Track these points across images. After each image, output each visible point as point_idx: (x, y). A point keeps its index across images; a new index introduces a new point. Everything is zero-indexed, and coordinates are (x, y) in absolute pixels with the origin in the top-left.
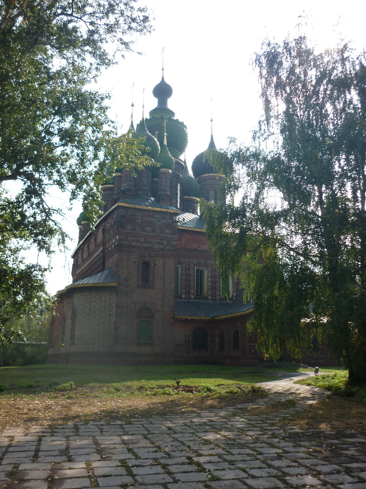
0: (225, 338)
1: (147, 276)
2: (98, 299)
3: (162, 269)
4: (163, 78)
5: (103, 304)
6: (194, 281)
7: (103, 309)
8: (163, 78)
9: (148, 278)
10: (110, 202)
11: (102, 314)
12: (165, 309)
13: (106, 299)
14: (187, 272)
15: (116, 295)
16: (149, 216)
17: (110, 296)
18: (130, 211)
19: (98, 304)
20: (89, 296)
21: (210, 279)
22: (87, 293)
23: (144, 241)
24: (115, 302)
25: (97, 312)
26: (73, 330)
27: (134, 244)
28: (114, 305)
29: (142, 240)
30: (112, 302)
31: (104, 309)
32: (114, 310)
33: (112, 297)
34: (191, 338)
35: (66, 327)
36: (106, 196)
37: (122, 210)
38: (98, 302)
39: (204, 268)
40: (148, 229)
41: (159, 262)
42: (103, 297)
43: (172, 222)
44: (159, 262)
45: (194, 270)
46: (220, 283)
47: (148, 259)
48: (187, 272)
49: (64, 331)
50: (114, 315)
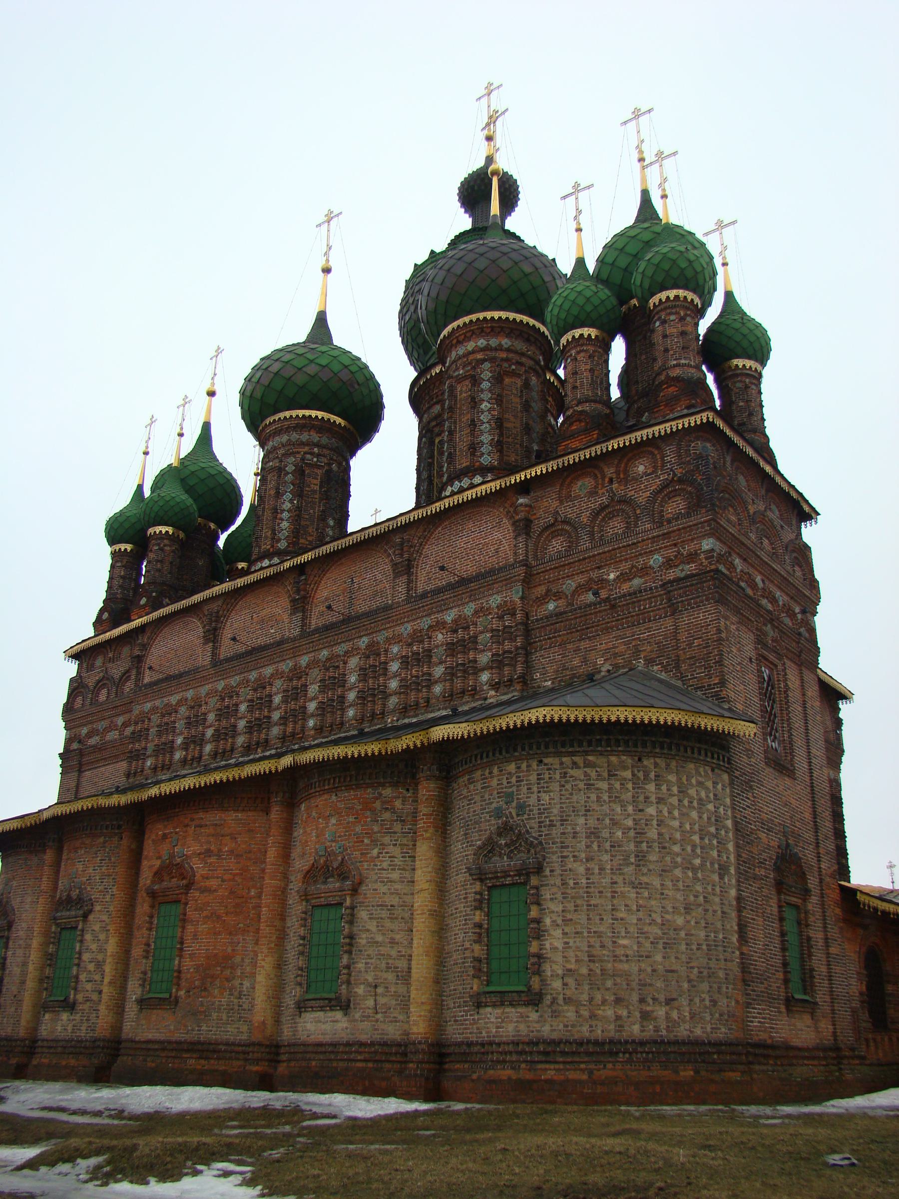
2: (675, 789)
5: (694, 814)
7: (696, 838)
10: (319, 472)
11: (697, 862)
15: (731, 783)
19: (676, 813)
20: (628, 774)
22: (613, 759)
25: (676, 848)
31: (701, 838)
32: (731, 846)
35: (363, 914)
36: (306, 449)
37: (708, 445)
38: (674, 801)
42: (694, 781)
49: (351, 937)
50: (732, 871)
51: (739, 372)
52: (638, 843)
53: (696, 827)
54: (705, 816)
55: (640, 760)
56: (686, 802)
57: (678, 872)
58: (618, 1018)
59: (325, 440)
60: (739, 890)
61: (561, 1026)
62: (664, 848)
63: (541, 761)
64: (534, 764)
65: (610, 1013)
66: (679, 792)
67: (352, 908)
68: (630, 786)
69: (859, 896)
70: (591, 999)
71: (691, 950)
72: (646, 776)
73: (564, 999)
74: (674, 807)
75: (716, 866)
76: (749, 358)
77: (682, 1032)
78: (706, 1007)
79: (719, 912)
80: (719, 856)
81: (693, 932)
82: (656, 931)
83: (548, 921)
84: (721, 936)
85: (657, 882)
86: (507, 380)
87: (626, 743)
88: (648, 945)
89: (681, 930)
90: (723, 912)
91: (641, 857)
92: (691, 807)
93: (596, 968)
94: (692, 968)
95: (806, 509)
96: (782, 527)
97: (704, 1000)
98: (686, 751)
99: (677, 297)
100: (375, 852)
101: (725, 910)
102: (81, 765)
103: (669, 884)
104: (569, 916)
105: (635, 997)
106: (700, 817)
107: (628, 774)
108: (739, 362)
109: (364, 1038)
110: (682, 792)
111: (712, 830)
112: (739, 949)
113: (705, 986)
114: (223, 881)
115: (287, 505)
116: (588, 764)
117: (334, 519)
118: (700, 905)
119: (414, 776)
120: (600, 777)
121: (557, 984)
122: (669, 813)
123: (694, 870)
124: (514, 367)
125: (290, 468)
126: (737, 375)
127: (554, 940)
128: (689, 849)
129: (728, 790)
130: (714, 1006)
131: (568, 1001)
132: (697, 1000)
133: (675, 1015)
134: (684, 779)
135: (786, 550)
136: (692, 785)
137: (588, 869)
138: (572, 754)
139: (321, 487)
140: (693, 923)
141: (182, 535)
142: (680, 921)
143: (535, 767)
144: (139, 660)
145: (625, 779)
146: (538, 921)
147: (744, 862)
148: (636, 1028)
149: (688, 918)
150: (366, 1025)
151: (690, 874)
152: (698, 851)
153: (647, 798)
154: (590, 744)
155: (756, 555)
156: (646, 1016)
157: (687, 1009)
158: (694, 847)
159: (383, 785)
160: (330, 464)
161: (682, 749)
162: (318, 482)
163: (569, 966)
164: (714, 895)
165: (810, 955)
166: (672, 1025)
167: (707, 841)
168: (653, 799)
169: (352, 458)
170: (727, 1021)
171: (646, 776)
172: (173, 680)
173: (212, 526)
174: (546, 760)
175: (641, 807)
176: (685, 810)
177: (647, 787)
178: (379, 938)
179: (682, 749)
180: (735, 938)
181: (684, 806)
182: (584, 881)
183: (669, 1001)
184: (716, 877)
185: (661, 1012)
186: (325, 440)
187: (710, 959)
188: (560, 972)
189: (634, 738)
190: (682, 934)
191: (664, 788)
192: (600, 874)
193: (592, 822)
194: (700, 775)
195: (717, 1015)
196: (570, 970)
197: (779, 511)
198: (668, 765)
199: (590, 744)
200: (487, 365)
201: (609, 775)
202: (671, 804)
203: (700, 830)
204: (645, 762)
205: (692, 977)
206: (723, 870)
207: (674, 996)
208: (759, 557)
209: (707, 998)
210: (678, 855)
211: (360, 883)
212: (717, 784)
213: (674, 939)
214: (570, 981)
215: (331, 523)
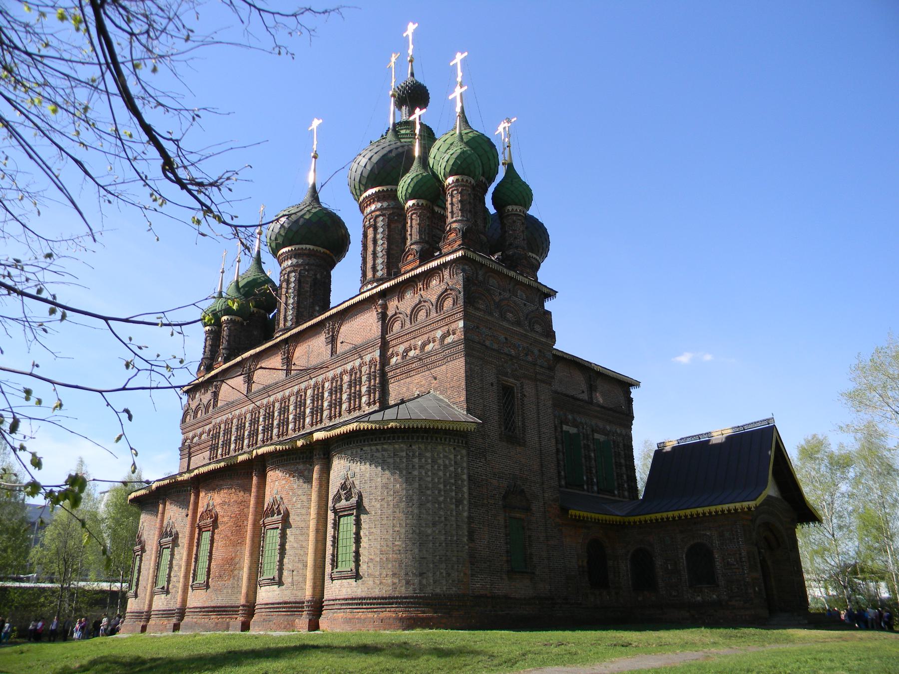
2: (430, 461)
3: (534, 407)
4: (412, 75)
5: (441, 474)
7: (441, 486)
11: (441, 499)
13: (447, 462)
15: (468, 454)
17: (455, 456)
19: (430, 473)
22: (397, 446)
24: (465, 471)
25: (429, 492)
27: (488, 343)
28: (465, 477)
29: (502, 338)
30: (459, 470)
31: (445, 486)
32: (465, 489)
34: (585, 564)
37: (466, 267)
38: (429, 467)
40: (509, 315)
41: (529, 389)
50: (465, 502)
51: (510, 213)
53: (442, 480)
54: (448, 474)
55: (411, 446)
57: (429, 505)
60: (469, 513)
61: (366, 589)
62: (422, 492)
63: (362, 449)
64: (359, 450)
66: (432, 462)
68: (404, 460)
70: (381, 574)
71: (436, 546)
72: (413, 455)
73: (368, 575)
75: (454, 500)
76: (516, 204)
78: (443, 577)
79: (455, 526)
80: (456, 495)
81: (437, 537)
84: (455, 538)
86: (393, 226)
87: (403, 438)
89: (429, 536)
90: (457, 525)
92: (439, 469)
94: (436, 556)
95: (546, 291)
96: (525, 305)
97: (442, 573)
98: (437, 440)
100: (294, 499)
101: (459, 524)
102: (190, 454)
103: (424, 511)
104: (372, 530)
106: (445, 475)
107: (404, 454)
108: (510, 208)
110: (434, 461)
111: (453, 481)
112: (467, 545)
113: (443, 566)
114: (231, 517)
117: (319, 306)
118: (442, 522)
119: (311, 458)
120: (390, 457)
122: (426, 473)
123: (439, 503)
124: (396, 218)
125: (293, 279)
126: (508, 215)
128: (436, 492)
129: (465, 459)
130: (449, 576)
132: (438, 573)
133: (424, 582)
134: (435, 455)
135: (526, 318)
136: (440, 458)
137: (381, 505)
138: (376, 445)
139: (311, 289)
140: (437, 532)
142: (429, 531)
143: (359, 452)
144: (216, 395)
145: (402, 457)
147: (474, 497)
149: (434, 529)
151: (437, 506)
152: (443, 493)
153: (413, 466)
154: (384, 440)
155: (500, 324)
157: (432, 578)
158: (440, 491)
159: (298, 463)
160: (315, 275)
161: (434, 439)
162: (308, 286)
163: (371, 557)
164: (451, 516)
167: (448, 487)
168: (417, 466)
169: (331, 270)
170: (457, 584)
171: (413, 455)
172: (230, 405)
173: (262, 311)
174: (364, 449)
175: (410, 471)
176: (435, 472)
177: (414, 460)
178: (295, 545)
179: (434, 439)
180: (465, 539)
181: (435, 469)
182: (380, 512)
184: (453, 507)
187: (447, 551)
188: (366, 560)
189: (407, 435)
190: (431, 538)
191: (423, 460)
192: (387, 507)
194: (446, 452)
195: (450, 581)
196: (371, 559)
197: (526, 295)
198: (426, 448)
199: (384, 440)
200: (381, 218)
201: (394, 455)
202: (427, 469)
203: (444, 481)
204: (413, 447)
205: (435, 561)
206: (459, 502)
207: (424, 572)
208: (502, 325)
209: (444, 572)
210: (430, 496)
212: (458, 456)
213: (426, 541)
214: (370, 564)
215: (317, 308)
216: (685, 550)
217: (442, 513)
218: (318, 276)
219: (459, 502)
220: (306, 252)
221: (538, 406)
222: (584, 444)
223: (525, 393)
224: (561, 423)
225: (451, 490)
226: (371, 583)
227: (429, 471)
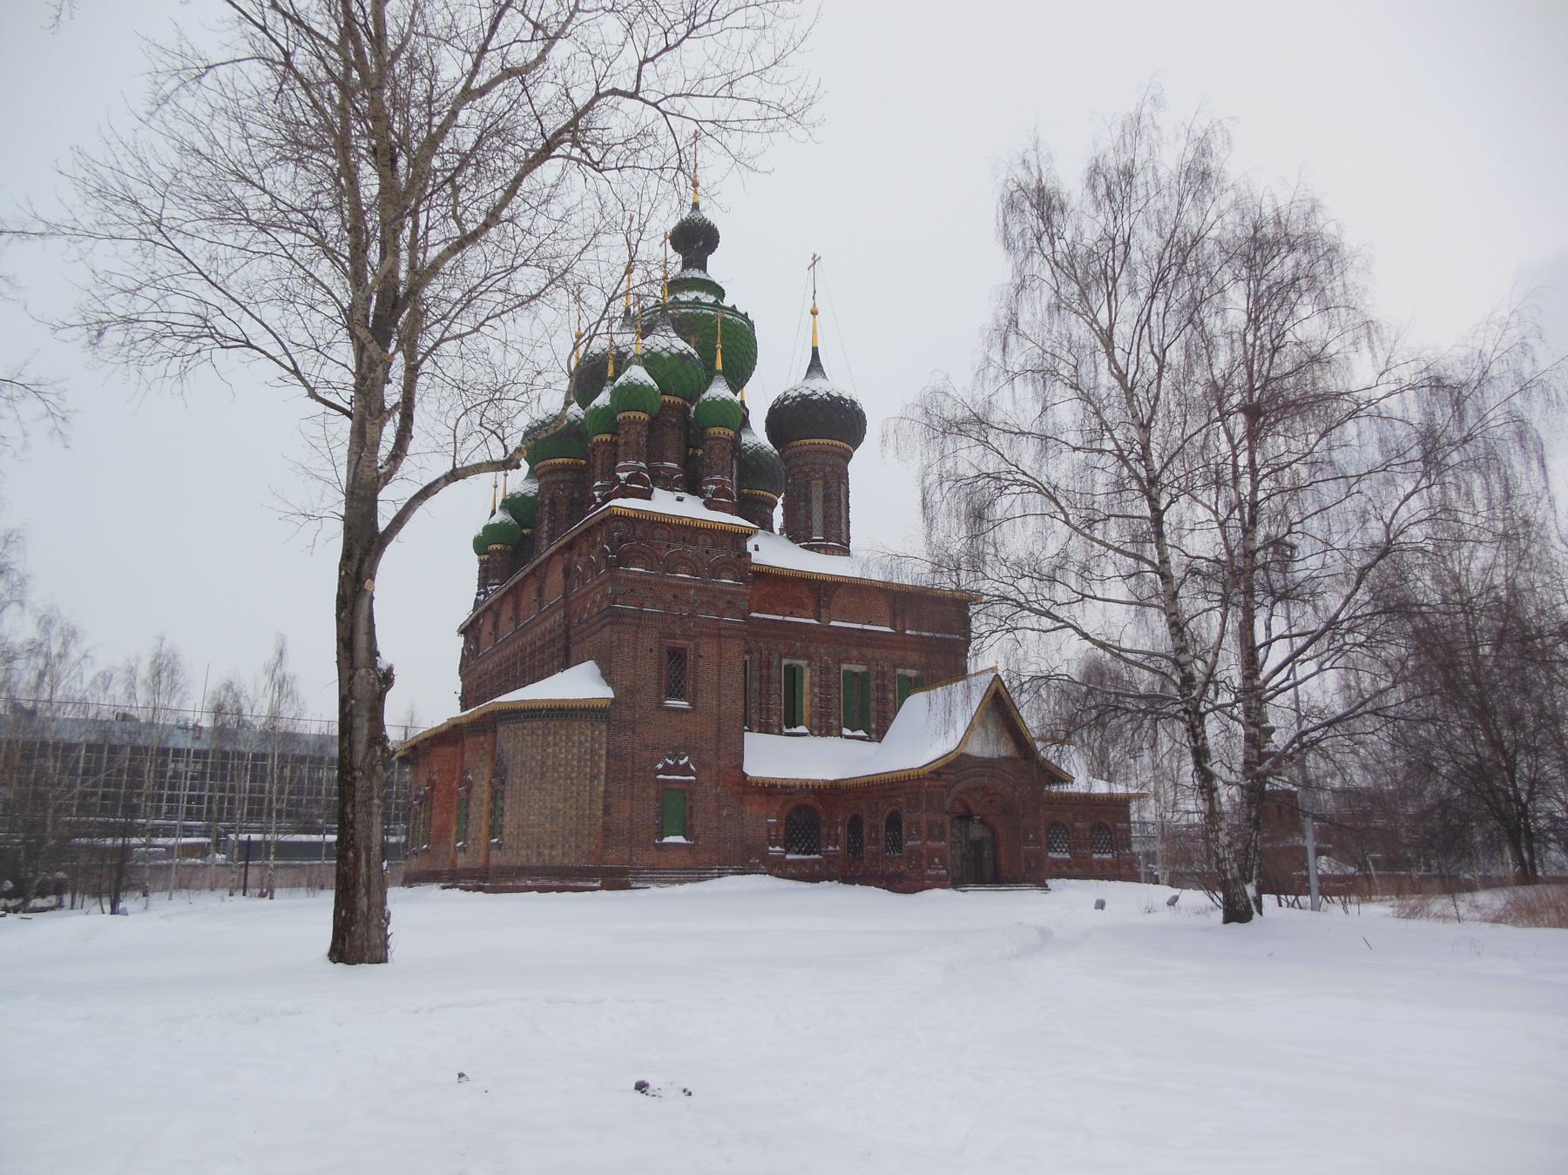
0: (866, 831)
1: (680, 682)
2: (564, 738)
3: (715, 667)
5: (575, 750)
6: (780, 696)
7: (575, 763)
8: (695, 206)
9: (682, 687)
11: (574, 775)
12: (722, 763)
13: (583, 738)
14: (764, 671)
15: (609, 730)
16: (684, 540)
17: (593, 732)
18: (639, 527)
20: (540, 732)
21: (816, 690)
22: (534, 724)
23: (672, 598)
24: (604, 746)
25: (562, 769)
26: (495, 812)
28: (603, 752)
32: (603, 764)
33: (597, 732)
34: (782, 833)
35: (472, 804)
37: (620, 523)
38: (563, 744)
39: (803, 663)
41: (708, 649)
43: (739, 556)
44: (708, 649)
45: (781, 668)
46: (839, 700)
47: (680, 643)
48: (764, 671)
49: (467, 816)
50: (602, 777)
52: (542, 768)
53: (576, 757)
56: (570, 744)
58: (527, 855)
59: (568, 477)
65: (523, 852)
67: (468, 800)
69: (748, 779)
74: (562, 747)
77: (557, 862)
79: (588, 800)
82: (548, 812)
83: (505, 809)
85: (549, 787)
88: (543, 819)
91: (543, 775)
92: (573, 746)
93: (520, 830)
99: (624, 418)
103: (556, 787)
105: (535, 845)
106: (579, 751)
107: (540, 732)
109: (470, 866)
110: (568, 738)
111: (588, 757)
113: (574, 838)
115: (546, 528)
116: (525, 728)
121: (506, 839)
123: (572, 779)
125: (547, 502)
126: (707, 440)
127: (507, 819)
129: (605, 734)
131: (510, 847)
141: (509, 547)
146: (502, 809)
148: (535, 860)
150: (471, 859)
153: (548, 744)
156: (540, 854)
165: (691, 816)
166: (552, 858)
171: (549, 733)
180: (600, 813)
183: (551, 847)
184: (587, 782)
185: (547, 852)
186: (568, 477)
193: (523, 758)
211: (471, 787)
216: (885, 817)
217: (574, 788)
218: (576, 495)
219: (593, 777)
220: (559, 467)
221: (719, 665)
222: (877, 684)
223: (702, 654)
224: (839, 662)
225: (585, 766)
226: (510, 854)
227: (562, 747)
